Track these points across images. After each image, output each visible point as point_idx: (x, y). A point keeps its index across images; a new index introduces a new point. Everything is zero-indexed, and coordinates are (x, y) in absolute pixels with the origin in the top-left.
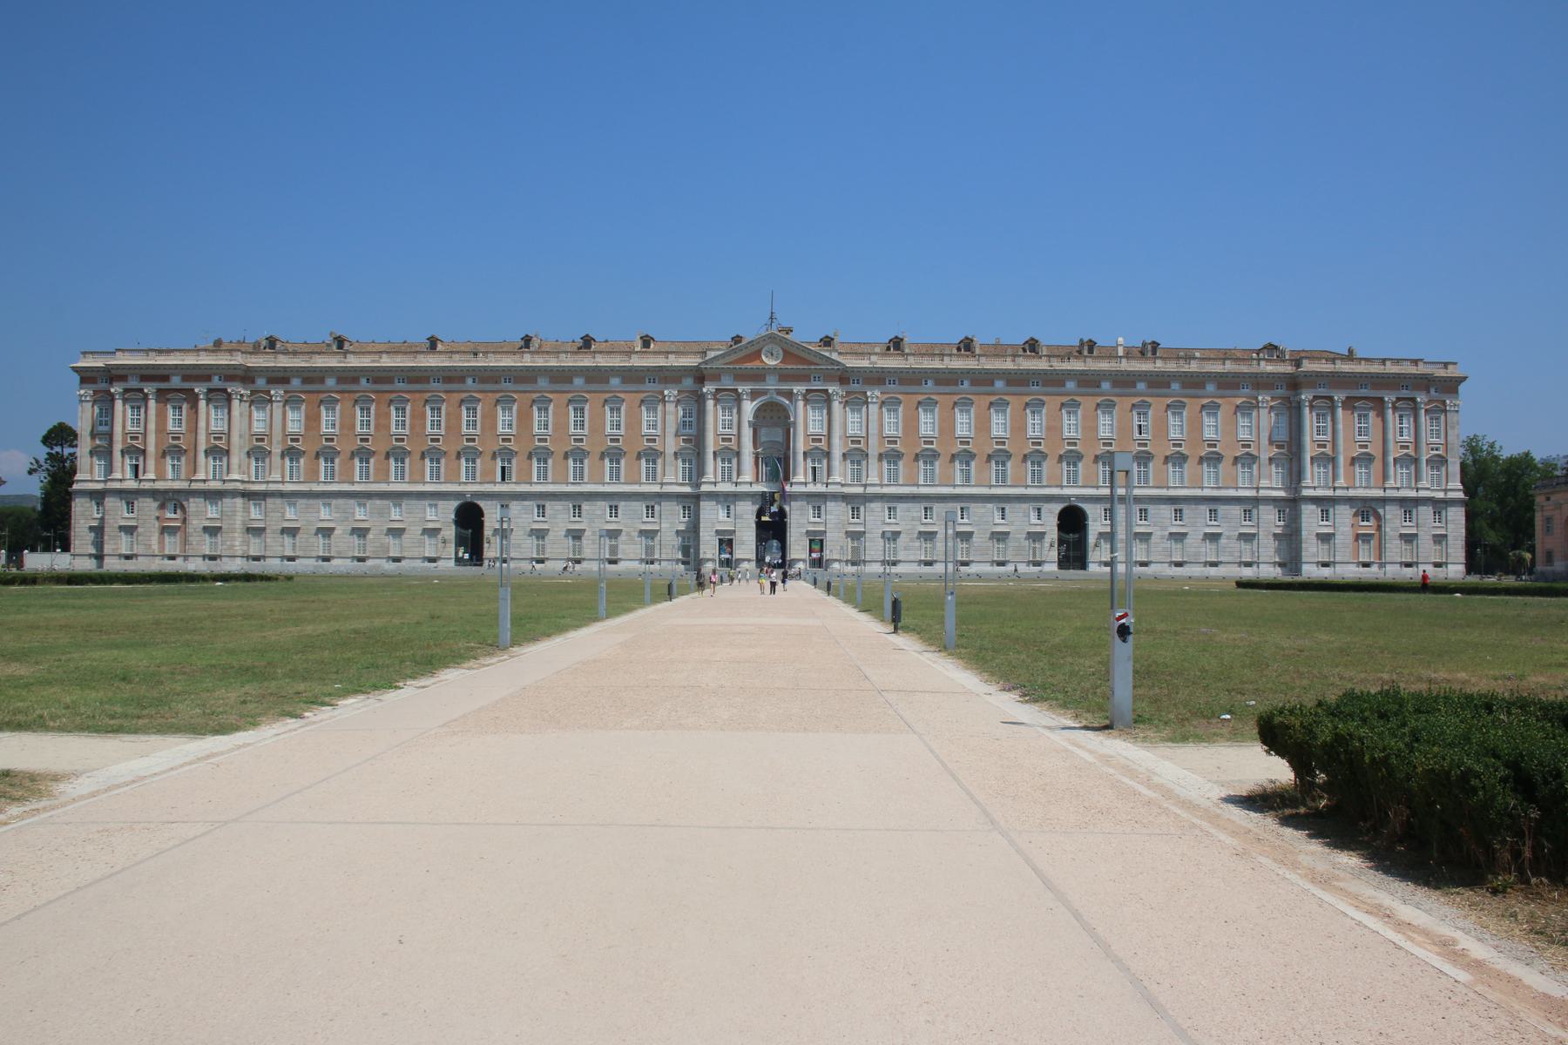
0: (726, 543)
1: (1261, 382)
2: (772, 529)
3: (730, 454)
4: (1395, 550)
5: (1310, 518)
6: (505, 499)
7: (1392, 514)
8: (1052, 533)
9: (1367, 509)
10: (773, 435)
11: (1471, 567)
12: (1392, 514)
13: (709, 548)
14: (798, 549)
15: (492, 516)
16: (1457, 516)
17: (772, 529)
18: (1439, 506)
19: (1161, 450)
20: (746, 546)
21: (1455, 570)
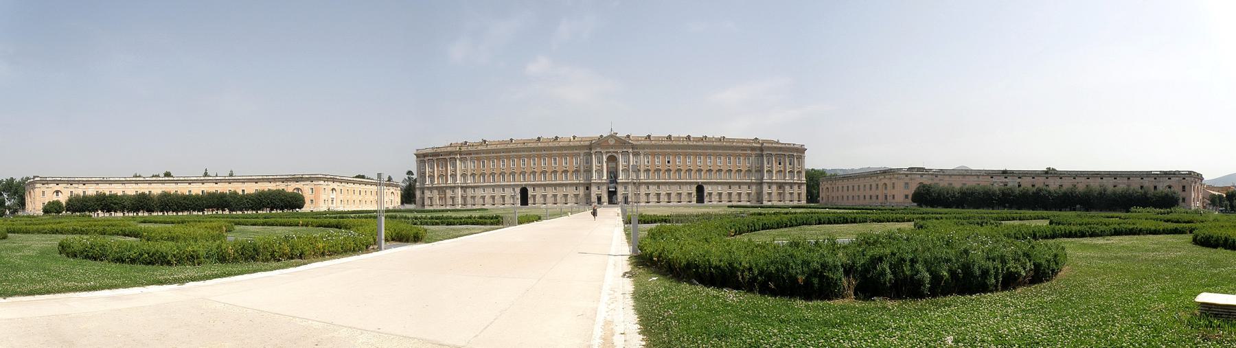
0: (599, 199)
1: (753, 149)
2: (612, 195)
3: (600, 171)
4: (788, 197)
5: (766, 189)
6: (534, 186)
7: (787, 187)
8: (694, 193)
9: (781, 186)
10: (612, 165)
11: (808, 201)
12: (787, 187)
13: (594, 198)
14: (620, 197)
15: (530, 192)
16: (804, 188)
17: (612, 195)
18: (800, 185)
19: (734, 170)
20: (605, 198)
21: (804, 202)
